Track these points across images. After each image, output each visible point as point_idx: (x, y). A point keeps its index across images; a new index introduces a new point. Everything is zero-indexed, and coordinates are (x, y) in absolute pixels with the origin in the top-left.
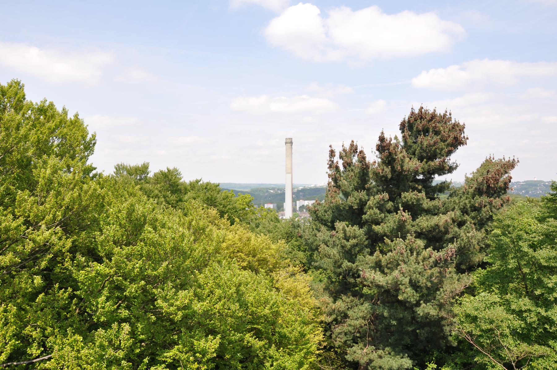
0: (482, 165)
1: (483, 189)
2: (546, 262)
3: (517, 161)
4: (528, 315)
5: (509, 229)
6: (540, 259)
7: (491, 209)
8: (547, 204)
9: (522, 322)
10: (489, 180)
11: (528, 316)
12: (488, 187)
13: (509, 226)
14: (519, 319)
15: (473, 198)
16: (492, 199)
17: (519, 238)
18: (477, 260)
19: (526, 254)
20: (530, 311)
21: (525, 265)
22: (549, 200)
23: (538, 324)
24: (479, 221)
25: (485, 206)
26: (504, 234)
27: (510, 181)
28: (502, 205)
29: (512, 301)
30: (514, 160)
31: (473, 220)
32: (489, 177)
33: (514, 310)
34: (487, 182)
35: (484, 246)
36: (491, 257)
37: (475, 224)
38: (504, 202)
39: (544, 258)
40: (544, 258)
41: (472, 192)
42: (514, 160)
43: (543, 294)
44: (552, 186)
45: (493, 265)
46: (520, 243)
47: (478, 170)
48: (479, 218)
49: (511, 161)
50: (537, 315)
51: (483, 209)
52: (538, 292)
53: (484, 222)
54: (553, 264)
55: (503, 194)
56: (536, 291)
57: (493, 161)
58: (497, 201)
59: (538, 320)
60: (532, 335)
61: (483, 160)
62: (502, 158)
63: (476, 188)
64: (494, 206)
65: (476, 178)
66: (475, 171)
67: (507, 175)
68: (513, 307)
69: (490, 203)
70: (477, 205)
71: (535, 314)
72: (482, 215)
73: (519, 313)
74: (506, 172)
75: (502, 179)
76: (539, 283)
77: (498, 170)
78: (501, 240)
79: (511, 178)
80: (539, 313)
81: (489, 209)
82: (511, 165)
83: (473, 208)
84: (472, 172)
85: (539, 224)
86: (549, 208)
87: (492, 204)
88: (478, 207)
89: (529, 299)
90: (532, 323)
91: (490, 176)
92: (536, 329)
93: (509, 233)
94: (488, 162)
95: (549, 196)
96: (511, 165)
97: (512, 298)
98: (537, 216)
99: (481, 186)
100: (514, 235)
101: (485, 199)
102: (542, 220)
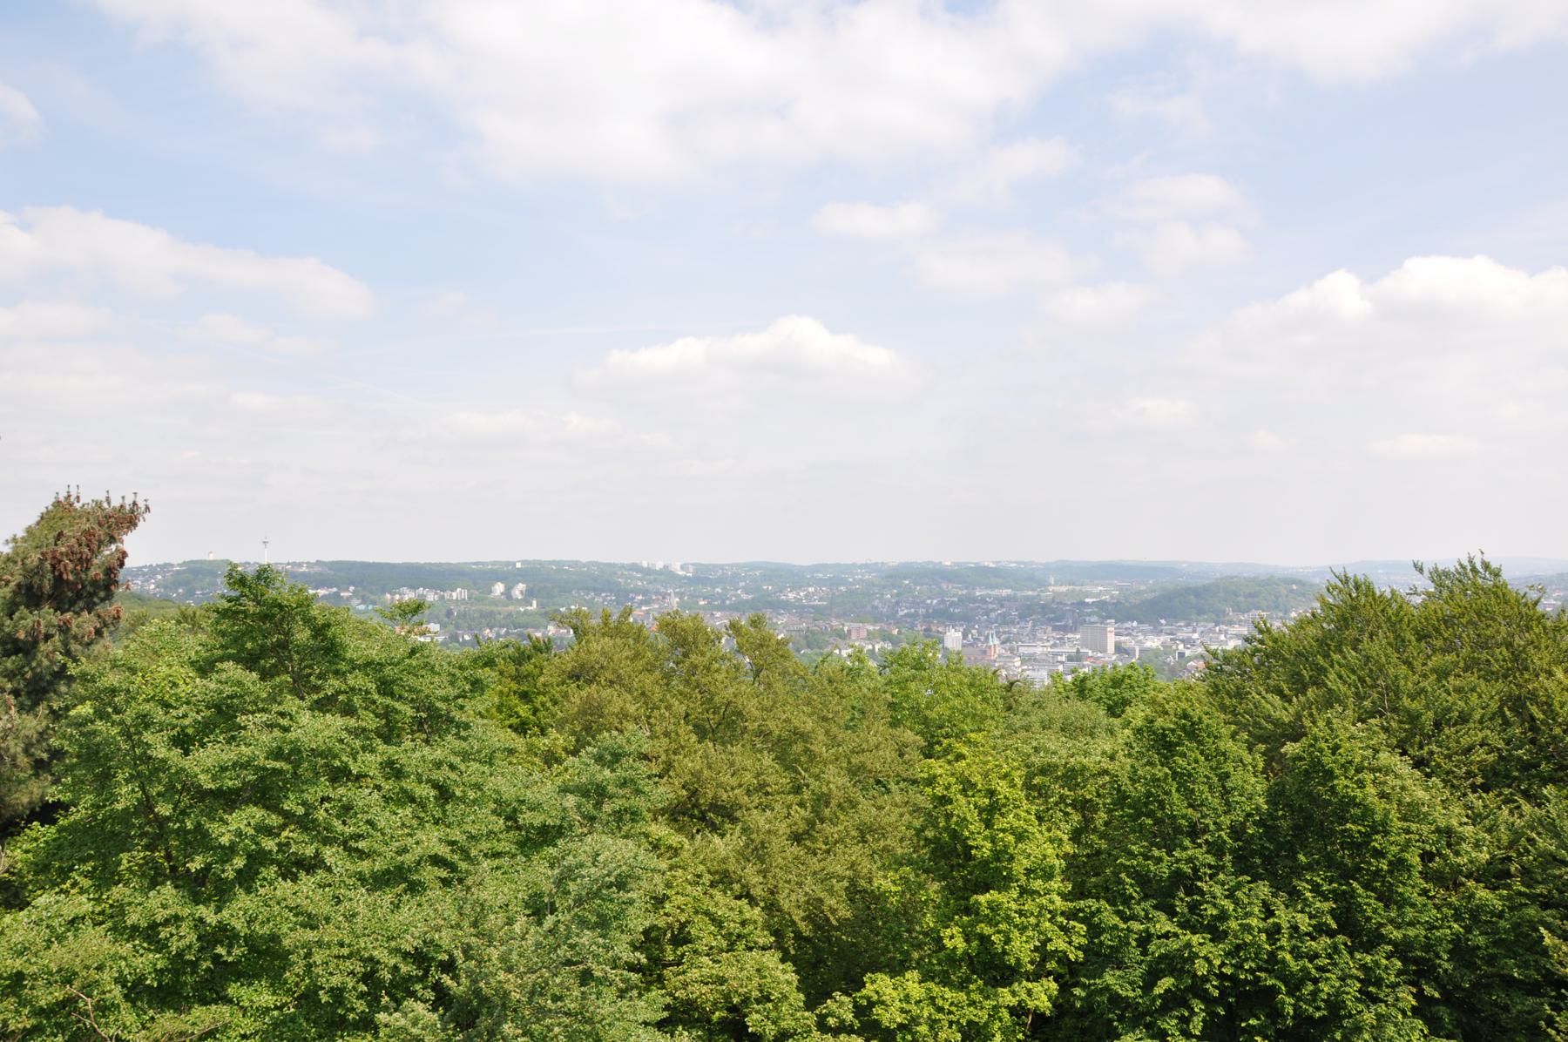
0: (42, 518)
1: (40, 588)
2: (214, 779)
3: (143, 508)
4: (174, 931)
5: (116, 699)
7: (65, 644)
9: (158, 956)
10: (60, 561)
11: (172, 935)
12: (59, 580)
13: (113, 691)
14: (149, 950)
15: (10, 616)
16: (68, 615)
17: (145, 721)
18: (25, 800)
19: (163, 765)
20: (177, 918)
21: (159, 794)
22: (224, 614)
23: (199, 951)
24: (28, 682)
25: (48, 637)
26: (101, 714)
27: (122, 564)
28: (99, 633)
29: (130, 904)
30: (135, 504)
31: (10, 680)
32: (61, 554)
33: (135, 928)
34: (53, 566)
35: (45, 756)
36: (67, 788)
37: (16, 693)
38: (105, 625)
39: (208, 771)
40: (208, 771)
41: (9, 596)
42: (135, 504)
43: (208, 868)
44: (230, 576)
45: (73, 809)
46: (148, 737)
47: (29, 531)
48: (28, 676)
49: (128, 508)
50: (195, 926)
51: (42, 647)
52: (196, 865)
53: (44, 684)
54: (230, 783)
55: (103, 600)
56: (193, 861)
57: (78, 506)
58: (84, 622)
59: (199, 939)
61: (47, 502)
62: (104, 499)
63: (19, 586)
64: (75, 637)
65: (21, 555)
66: (21, 534)
67: (113, 547)
68: (133, 918)
69: (64, 629)
70: (22, 635)
71: (192, 924)
72: (39, 664)
73: (150, 934)
74: (112, 540)
75: (95, 561)
76: (199, 840)
77: (87, 533)
78: (94, 733)
79: (124, 554)
80: (201, 920)
81: (59, 644)
82: (127, 519)
83: (9, 646)
84: (9, 537)
86: (223, 634)
87: (68, 629)
88: (25, 642)
89: (176, 887)
90: (184, 951)
91: (63, 549)
92: (194, 965)
93: (117, 711)
94: (62, 510)
95: (226, 605)
96: (127, 519)
97: (128, 893)
98: (194, 658)
99: (36, 580)
100: (129, 716)
101: (47, 617)
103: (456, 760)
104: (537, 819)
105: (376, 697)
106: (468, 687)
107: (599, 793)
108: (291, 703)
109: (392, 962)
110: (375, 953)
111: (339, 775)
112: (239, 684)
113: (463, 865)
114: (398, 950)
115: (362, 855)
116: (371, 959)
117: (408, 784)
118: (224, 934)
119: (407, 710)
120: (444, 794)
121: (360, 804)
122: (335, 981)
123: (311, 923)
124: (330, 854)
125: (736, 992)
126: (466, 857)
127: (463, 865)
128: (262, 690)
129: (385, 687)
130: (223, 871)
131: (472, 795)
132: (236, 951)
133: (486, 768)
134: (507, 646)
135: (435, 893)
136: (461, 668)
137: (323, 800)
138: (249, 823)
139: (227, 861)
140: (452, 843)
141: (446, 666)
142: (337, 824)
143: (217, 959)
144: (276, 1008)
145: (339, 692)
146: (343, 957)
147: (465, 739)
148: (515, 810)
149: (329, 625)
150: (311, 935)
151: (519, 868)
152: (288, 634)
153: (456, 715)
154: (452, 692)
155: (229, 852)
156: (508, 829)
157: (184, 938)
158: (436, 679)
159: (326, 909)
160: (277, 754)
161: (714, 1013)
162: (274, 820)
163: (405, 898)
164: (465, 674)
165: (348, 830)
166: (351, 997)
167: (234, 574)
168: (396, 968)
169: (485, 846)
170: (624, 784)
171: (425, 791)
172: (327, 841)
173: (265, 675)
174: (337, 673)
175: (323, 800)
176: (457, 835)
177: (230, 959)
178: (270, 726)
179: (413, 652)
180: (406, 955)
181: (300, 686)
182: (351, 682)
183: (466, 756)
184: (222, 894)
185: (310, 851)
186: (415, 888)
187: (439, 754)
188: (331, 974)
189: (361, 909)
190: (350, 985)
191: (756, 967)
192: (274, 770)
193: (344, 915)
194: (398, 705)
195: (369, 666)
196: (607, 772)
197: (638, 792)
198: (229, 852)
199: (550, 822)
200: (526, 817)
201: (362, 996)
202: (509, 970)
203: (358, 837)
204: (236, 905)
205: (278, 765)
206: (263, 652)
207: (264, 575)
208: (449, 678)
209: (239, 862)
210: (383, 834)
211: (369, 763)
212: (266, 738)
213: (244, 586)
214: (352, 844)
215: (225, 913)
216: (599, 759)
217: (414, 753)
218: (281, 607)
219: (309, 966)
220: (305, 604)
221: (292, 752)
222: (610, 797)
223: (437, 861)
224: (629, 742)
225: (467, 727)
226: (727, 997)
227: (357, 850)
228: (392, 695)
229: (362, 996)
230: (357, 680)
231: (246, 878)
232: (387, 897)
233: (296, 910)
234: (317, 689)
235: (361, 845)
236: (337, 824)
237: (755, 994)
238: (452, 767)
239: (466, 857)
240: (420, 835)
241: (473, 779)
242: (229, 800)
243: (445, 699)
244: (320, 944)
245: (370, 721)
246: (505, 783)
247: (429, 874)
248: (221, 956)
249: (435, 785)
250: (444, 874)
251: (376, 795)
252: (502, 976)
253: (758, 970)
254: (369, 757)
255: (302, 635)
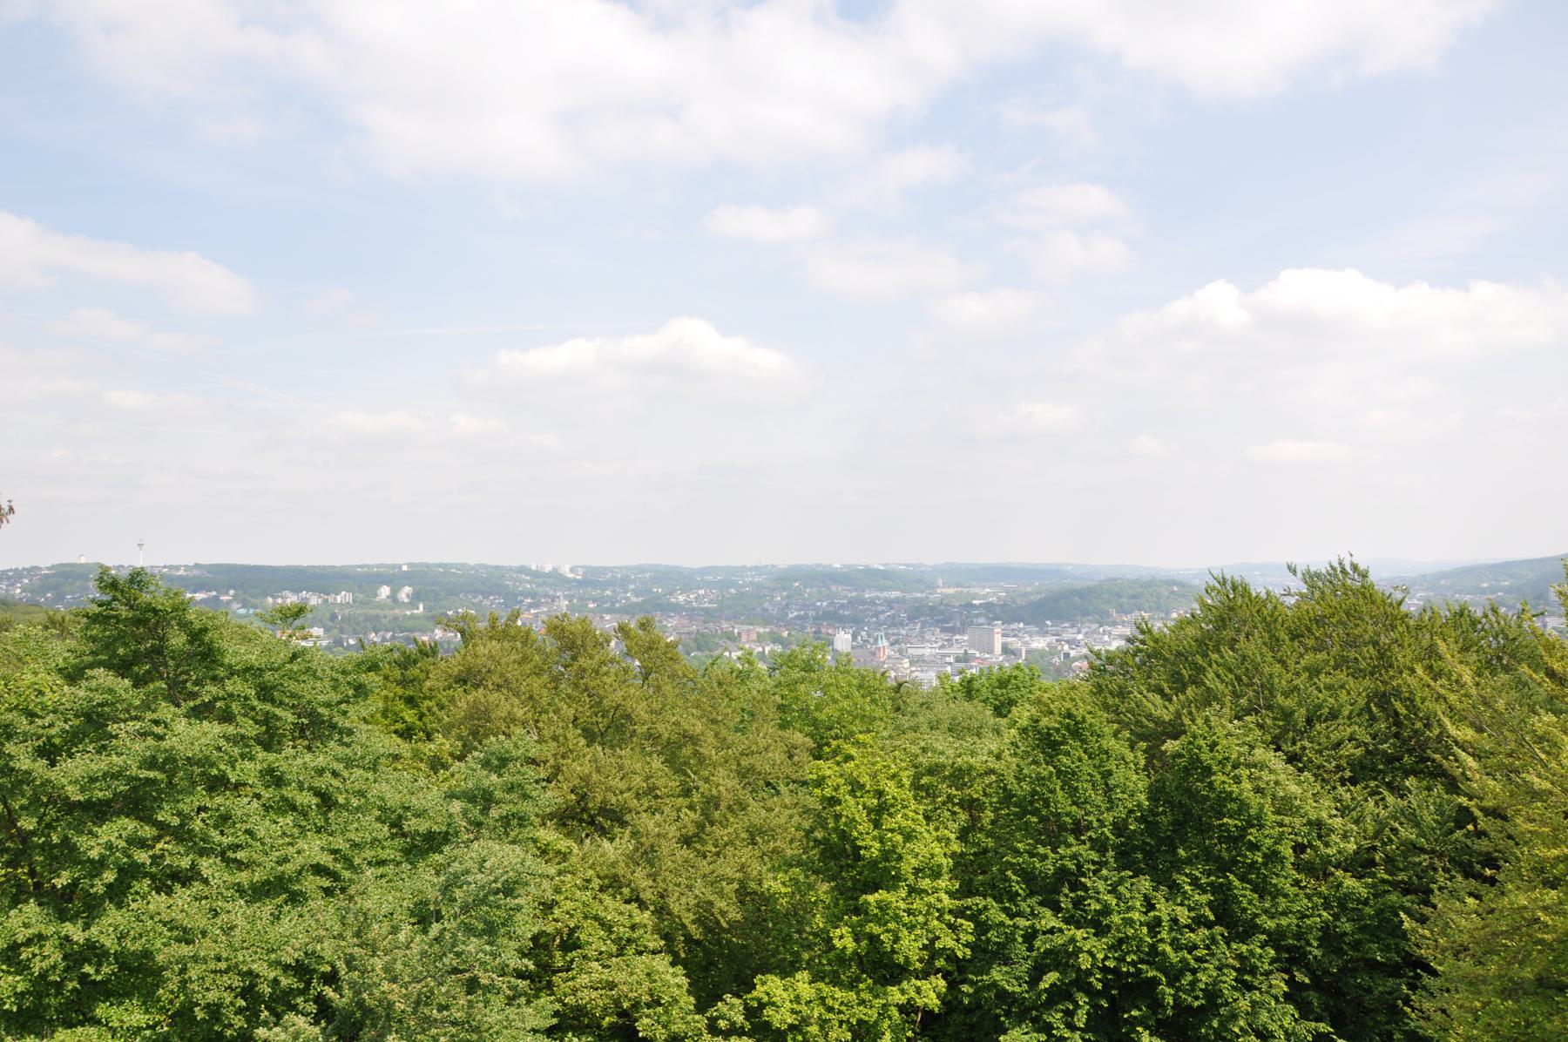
3: (7, 509)
4: (37, 951)
6: (63, 787)
8: (87, 628)
11: (34, 955)
21: (22, 808)
22: (94, 619)
39: (76, 782)
40: (76, 782)
43: (74, 884)
44: (101, 579)
50: (61, 944)
52: (62, 880)
54: (100, 795)
56: (59, 876)
59: (65, 958)
60: (49, 1006)
71: (57, 943)
76: (67, 854)
80: (67, 938)
85: (66, 688)
86: (94, 639)
89: (39, 905)
90: (47, 971)
92: (59, 986)
98: (62, 665)
102: (73, 676)
103: (339, 767)
104: (423, 826)
105: (256, 703)
106: (351, 692)
107: (485, 799)
108: (165, 711)
109: (272, 975)
110: (254, 966)
111: (217, 784)
112: (111, 691)
113: (346, 874)
114: (278, 963)
115: (240, 865)
116: (250, 973)
117: (289, 792)
118: (93, 951)
119: (288, 716)
120: (326, 801)
121: (239, 813)
122: (212, 996)
123: (186, 937)
124: (206, 865)
125: (626, 996)
126: (350, 866)
127: (346, 874)
128: (136, 697)
129: (265, 693)
130: (92, 886)
131: (355, 802)
132: (106, 970)
133: (370, 775)
134: (392, 650)
135: (317, 903)
136: (344, 672)
137: (200, 809)
138: (120, 835)
139: (96, 876)
140: (335, 852)
141: (328, 671)
142: (215, 835)
143: (84, 979)
144: (149, 1027)
145: (216, 699)
146: (220, 971)
147: (348, 745)
148: (400, 817)
149: (205, 630)
150: (186, 950)
151: (404, 876)
152: (162, 639)
153: (339, 720)
154: (335, 697)
155: (98, 866)
156: (393, 837)
157: (53, 955)
158: (319, 684)
159: (202, 922)
160: (151, 763)
161: (603, 1019)
162: (148, 831)
163: (286, 908)
164: (348, 679)
165: (226, 841)
166: (229, 1013)
167: (105, 578)
168: (276, 981)
169: (369, 854)
170: (511, 789)
171: (306, 799)
172: (203, 853)
173: (138, 682)
174: (214, 679)
175: (200, 809)
176: (340, 843)
177: (99, 978)
178: (144, 735)
179: (294, 657)
180: (286, 968)
181: (176, 693)
182: (229, 688)
183: (349, 763)
184: (91, 910)
185: (185, 863)
186: (296, 898)
187: (321, 761)
188: (208, 989)
189: (240, 922)
190: (228, 1001)
191: (646, 971)
192: (147, 780)
193: (221, 928)
194: (278, 711)
195: (248, 671)
196: (494, 777)
197: (525, 797)
198: (98, 866)
199: (435, 828)
200: (411, 824)
201: (240, 1011)
202: (394, 980)
203: (236, 847)
204: (105, 921)
205: (151, 774)
206: (136, 658)
207: (137, 578)
208: (331, 683)
209: (110, 876)
210: (263, 844)
211: (248, 771)
212: (138, 746)
213: (116, 590)
214: (230, 854)
215: (94, 930)
216: (486, 764)
217: (295, 760)
218: (155, 611)
219: (184, 983)
220: (181, 608)
221: (166, 760)
222: (497, 803)
223: (319, 870)
224: (516, 746)
225: (350, 732)
226: (617, 1002)
227: (235, 860)
228: (273, 701)
229: (240, 1011)
230: (235, 686)
231: (117, 893)
232: (267, 909)
233: (171, 925)
234: (193, 695)
235: (240, 855)
236: (215, 835)
237: (646, 998)
238: (335, 774)
239: (350, 866)
240: (301, 844)
241: (357, 786)
242: (100, 811)
243: (328, 705)
244: (195, 959)
245: (250, 729)
246: (389, 789)
247: (311, 883)
248: (89, 975)
249: (318, 793)
250: (326, 883)
251: (255, 804)
252: (386, 986)
253: (648, 975)
254: (248, 765)
255: (177, 640)
